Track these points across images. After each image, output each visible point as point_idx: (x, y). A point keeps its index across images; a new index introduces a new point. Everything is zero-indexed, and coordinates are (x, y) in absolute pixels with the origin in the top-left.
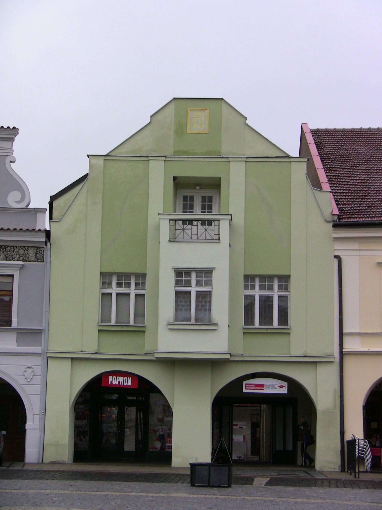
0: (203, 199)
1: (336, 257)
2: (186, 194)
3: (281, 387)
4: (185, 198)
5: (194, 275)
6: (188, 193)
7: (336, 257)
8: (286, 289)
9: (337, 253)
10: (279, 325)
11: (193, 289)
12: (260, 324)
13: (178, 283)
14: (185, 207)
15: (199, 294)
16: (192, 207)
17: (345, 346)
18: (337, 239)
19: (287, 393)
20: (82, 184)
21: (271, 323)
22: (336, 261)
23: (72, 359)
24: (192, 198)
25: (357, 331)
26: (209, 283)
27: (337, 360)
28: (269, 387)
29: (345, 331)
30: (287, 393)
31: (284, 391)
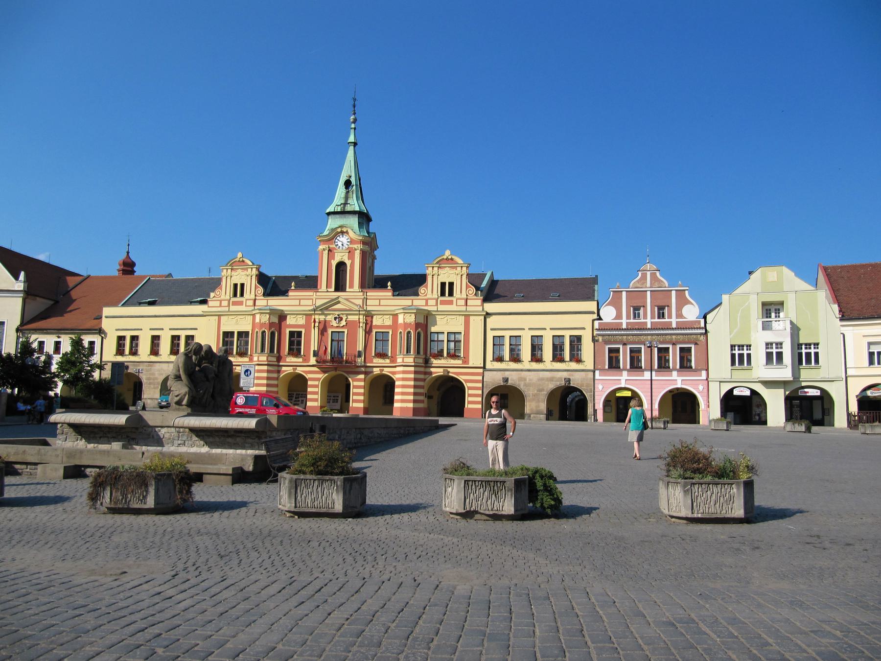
0: (776, 310)
1: (841, 333)
2: (767, 308)
3: (817, 392)
4: (767, 310)
5: (774, 345)
6: (768, 307)
7: (841, 333)
8: (818, 348)
9: (842, 332)
10: (815, 364)
11: (774, 351)
12: (806, 364)
13: (767, 348)
14: (767, 314)
15: (777, 353)
16: (770, 314)
17: (848, 373)
18: (842, 326)
19: (819, 394)
20: (719, 307)
21: (811, 363)
22: (842, 335)
23: (720, 382)
24: (770, 310)
25: (853, 366)
26: (782, 348)
27: (844, 379)
28: (811, 393)
29: (847, 367)
30: (819, 394)
31: (819, 394)
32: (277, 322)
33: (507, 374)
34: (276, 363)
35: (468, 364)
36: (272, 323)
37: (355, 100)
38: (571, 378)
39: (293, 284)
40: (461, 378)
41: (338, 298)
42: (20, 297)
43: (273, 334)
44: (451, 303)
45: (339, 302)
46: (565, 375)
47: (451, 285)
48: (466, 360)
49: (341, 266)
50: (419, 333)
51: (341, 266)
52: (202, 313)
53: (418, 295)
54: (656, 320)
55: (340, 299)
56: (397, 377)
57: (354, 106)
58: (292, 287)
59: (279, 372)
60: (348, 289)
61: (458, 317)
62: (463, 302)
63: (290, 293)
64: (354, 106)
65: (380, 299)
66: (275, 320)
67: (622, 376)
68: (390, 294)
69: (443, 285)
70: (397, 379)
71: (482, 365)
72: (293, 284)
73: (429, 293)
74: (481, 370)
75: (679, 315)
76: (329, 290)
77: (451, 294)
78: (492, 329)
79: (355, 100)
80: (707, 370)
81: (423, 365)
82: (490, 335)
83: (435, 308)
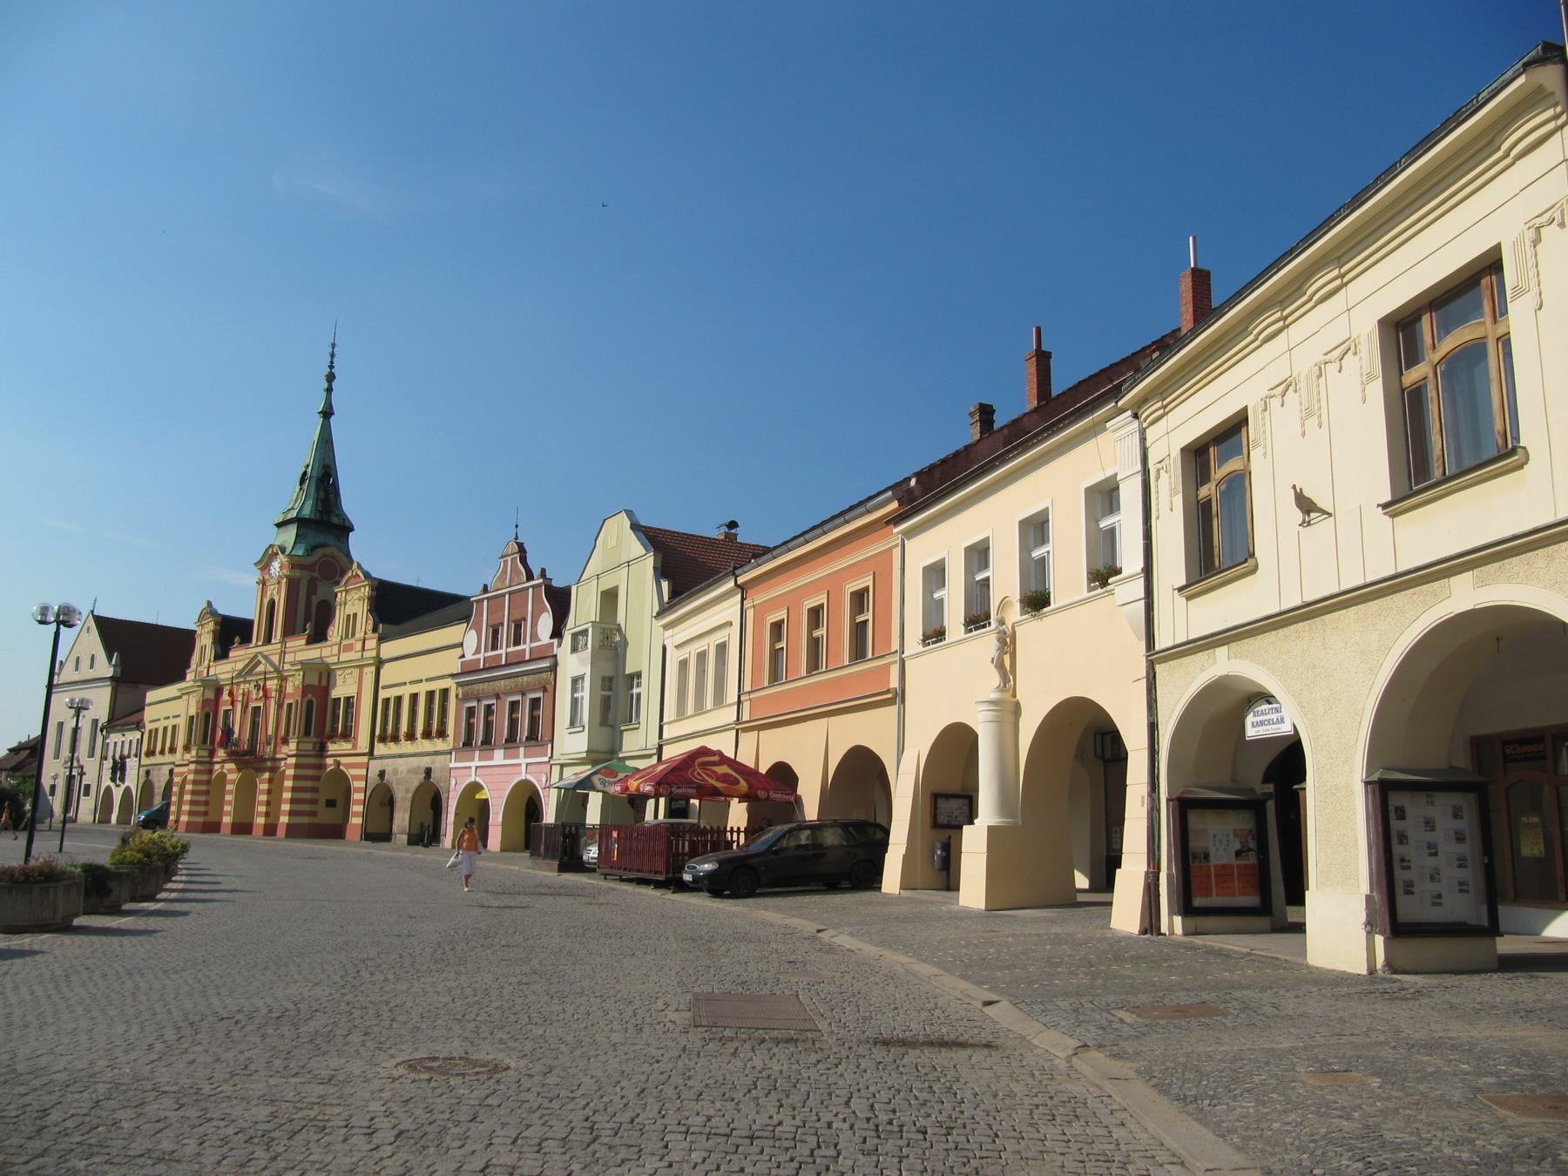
32: (213, 698)
33: (387, 765)
34: (208, 759)
35: (356, 749)
36: (207, 699)
37: (333, 345)
38: (433, 767)
39: (237, 639)
40: (351, 772)
41: (256, 656)
42: (109, 685)
43: (207, 715)
44: (349, 648)
45: (259, 663)
46: (426, 762)
47: (355, 615)
48: (355, 746)
49: (272, 604)
50: (310, 703)
51: (272, 604)
52: (178, 694)
53: (326, 639)
54: (512, 649)
55: (260, 658)
56: (352, 773)
57: (332, 356)
58: (234, 643)
59: (210, 772)
60: (273, 641)
61: (353, 669)
62: (359, 646)
63: (231, 654)
64: (332, 356)
65: (295, 652)
66: (211, 695)
67: (517, 757)
68: (304, 642)
69: (349, 616)
70: (352, 776)
71: (367, 750)
72: (237, 639)
73: (335, 632)
74: (365, 759)
75: (534, 637)
76: (260, 643)
77: (353, 635)
78: (383, 688)
79: (333, 345)
80: (552, 741)
81: (313, 753)
82: (383, 694)
83: (335, 659)
